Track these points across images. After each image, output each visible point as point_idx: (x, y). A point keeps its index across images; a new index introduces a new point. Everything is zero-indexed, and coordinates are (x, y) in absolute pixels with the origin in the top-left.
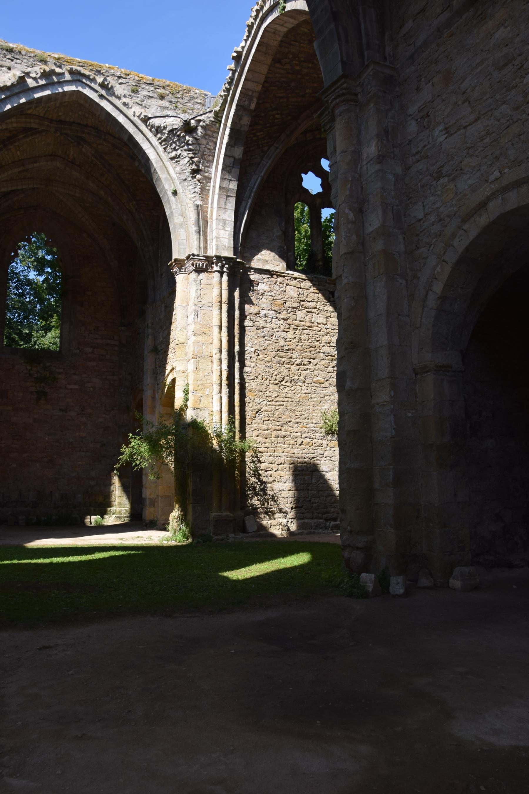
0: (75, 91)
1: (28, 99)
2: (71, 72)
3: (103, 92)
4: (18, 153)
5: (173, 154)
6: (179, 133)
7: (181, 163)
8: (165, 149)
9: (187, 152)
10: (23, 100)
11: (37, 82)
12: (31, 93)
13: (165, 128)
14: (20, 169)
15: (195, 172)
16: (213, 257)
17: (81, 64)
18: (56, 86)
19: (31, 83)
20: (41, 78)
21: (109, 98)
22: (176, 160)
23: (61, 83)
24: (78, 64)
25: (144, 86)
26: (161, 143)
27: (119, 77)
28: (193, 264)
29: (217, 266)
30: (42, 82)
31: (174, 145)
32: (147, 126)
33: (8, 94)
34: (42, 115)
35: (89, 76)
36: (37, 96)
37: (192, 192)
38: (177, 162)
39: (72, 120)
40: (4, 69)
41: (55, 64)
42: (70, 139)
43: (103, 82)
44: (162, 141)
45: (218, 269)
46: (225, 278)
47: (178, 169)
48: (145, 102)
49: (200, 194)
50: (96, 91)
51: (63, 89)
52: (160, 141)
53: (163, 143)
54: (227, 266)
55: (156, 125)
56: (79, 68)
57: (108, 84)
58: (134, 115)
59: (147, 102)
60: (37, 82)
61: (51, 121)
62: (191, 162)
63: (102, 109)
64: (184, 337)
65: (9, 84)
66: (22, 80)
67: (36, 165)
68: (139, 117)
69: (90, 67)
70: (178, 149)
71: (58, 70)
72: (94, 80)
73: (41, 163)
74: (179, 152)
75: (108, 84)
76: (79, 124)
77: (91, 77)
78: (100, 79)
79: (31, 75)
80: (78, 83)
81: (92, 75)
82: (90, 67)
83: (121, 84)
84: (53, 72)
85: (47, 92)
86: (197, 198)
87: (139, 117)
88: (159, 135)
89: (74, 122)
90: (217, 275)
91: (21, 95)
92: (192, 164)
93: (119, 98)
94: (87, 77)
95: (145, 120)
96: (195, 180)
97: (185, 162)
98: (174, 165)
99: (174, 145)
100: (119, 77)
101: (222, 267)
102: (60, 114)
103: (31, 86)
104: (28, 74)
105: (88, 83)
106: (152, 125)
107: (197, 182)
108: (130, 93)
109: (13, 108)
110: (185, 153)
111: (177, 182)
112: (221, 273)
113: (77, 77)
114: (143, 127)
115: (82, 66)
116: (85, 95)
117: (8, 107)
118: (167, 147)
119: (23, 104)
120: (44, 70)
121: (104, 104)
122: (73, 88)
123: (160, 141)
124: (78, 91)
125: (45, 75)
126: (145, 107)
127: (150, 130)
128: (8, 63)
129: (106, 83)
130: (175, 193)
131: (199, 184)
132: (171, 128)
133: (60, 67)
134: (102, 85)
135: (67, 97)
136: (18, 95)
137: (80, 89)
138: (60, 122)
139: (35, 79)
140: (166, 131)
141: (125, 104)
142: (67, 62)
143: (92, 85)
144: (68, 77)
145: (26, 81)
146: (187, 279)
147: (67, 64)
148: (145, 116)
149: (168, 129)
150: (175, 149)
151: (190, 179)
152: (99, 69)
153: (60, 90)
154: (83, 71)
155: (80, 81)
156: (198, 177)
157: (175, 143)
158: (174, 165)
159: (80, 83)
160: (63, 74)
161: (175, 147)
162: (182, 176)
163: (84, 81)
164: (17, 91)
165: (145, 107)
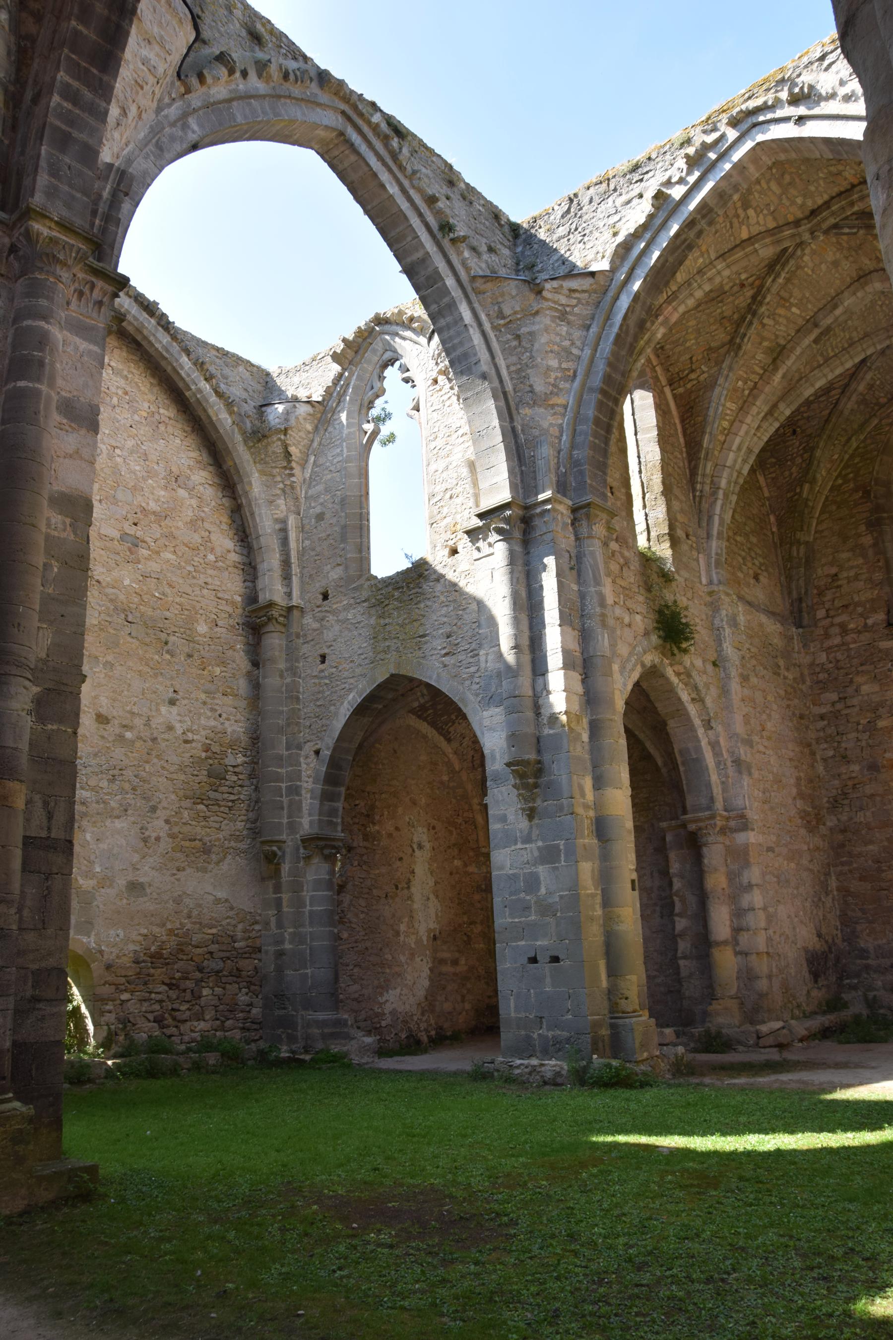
0: (753, 149)
1: (681, 221)
2: (734, 123)
4: (794, 310)
10: (674, 228)
11: (686, 183)
12: (682, 208)
14: (813, 336)
18: (719, 164)
19: (677, 192)
20: (689, 172)
21: (816, 111)
24: (742, 100)
33: (648, 235)
34: (771, 224)
35: (765, 103)
39: (826, 197)
40: (636, 201)
41: (705, 132)
42: (846, 230)
43: (791, 93)
51: (730, 162)
56: (744, 107)
57: (802, 88)
60: (686, 183)
61: (797, 223)
63: (812, 140)
65: (642, 220)
66: (660, 197)
67: (838, 312)
69: (764, 87)
71: (710, 139)
73: (846, 304)
75: (802, 88)
76: (840, 194)
77: (770, 103)
78: (784, 95)
79: (674, 180)
80: (754, 130)
81: (770, 98)
82: (764, 87)
84: (706, 147)
89: (832, 198)
91: (670, 223)
94: (764, 108)
102: (799, 201)
104: (668, 183)
105: (769, 116)
109: (665, 253)
113: (746, 120)
115: (749, 98)
116: (773, 141)
117: (656, 254)
119: (677, 235)
120: (687, 156)
122: (748, 145)
124: (758, 144)
125: (692, 162)
129: (797, 90)
133: (715, 129)
134: (794, 100)
135: (752, 168)
136: (664, 225)
137: (760, 138)
138: (814, 213)
139: (681, 181)
143: (779, 113)
144: (732, 134)
145: (670, 195)
153: (727, 166)
154: (752, 104)
155: (755, 125)
159: (757, 128)
160: (723, 136)
163: (761, 118)
164: (658, 221)
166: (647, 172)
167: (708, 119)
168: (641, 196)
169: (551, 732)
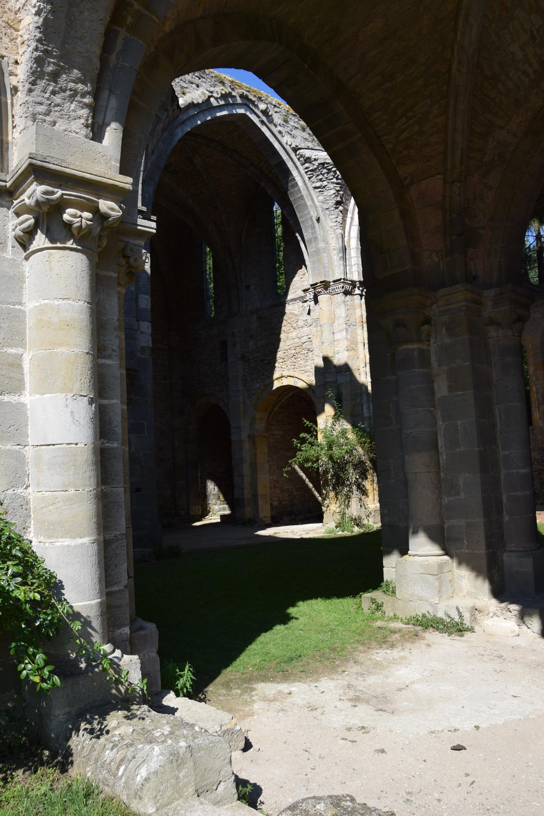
2: (242, 96)
3: (264, 119)
5: (318, 184)
6: (330, 167)
7: (326, 193)
8: (310, 178)
9: (335, 185)
13: (315, 160)
15: (338, 203)
16: (356, 282)
17: (248, 89)
22: (319, 190)
23: (235, 105)
25: (291, 117)
26: (306, 172)
27: (275, 106)
28: (343, 287)
29: (359, 289)
30: (222, 103)
31: (321, 177)
32: (296, 155)
35: (254, 101)
36: (218, 114)
37: (335, 220)
38: (320, 191)
44: (308, 171)
45: (359, 292)
46: (363, 300)
47: (321, 198)
48: (293, 132)
49: (341, 224)
50: (258, 117)
51: (236, 111)
52: (307, 170)
53: (309, 173)
54: (365, 290)
55: (307, 155)
58: (287, 144)
59: (294, 132)
62: (337, 194)
64: (332, 351)
68: (290, 145)
69: (254, 93)
70: (324, 181)
72: (256, 106)
74: (325, 183)
78: (262, 106)
82: (254, 93)
83: (276, 112)
85: (225, 113)
86: (338, 227)
87: (290, 145)
88: (307, 165)
90: (359, 297)
92: (337, 196)
93: (276, 126)
94: (253, 102)
95: (295, 150)
96: (337, 210)
97: (331, 194)
98: (317, 194)
99: (321, 177)
100: (275, 106)
101: (362, 291)
103: (214, 105)
106: (301, 156)
107: (340, 213)
108: (282, 122)
110: (332, 186)
111: (320, 209)
112: (361, 295)
114: (293, 155)
115: (248, 91)
118: (312, 177)
121: (264, 129)
122: (241, 111)
123: (307, 170)
125: (224, 96)
126: (294, 137)
127: (299, 159)
128: (197, 81)
130: (318, 220)
131: (341, 215)
132: (323, 162)
137: (248, 113)
139: (216, 99)
140: (316, 163)
141: (280, 132)
142: (238, 86)
143: (256, 110)
144: (239, 100)
146: (331, 299)
147: (238, 87)
148: (297, 146)
149: (319, 161)
150: (321, 180)
151: (333, 209)
152: (260, 96)
154: (251, 97)
155: (246, 105)
156: (341, 208)
157: (323, 175)
158: (317, 194)
161: (322, 179)
162: (324, 205)
163: (251, 106)
165: (294, 137)
166: (202, 77)
167: (232, 82)
168: (198, 86)
169: (142, 356)
